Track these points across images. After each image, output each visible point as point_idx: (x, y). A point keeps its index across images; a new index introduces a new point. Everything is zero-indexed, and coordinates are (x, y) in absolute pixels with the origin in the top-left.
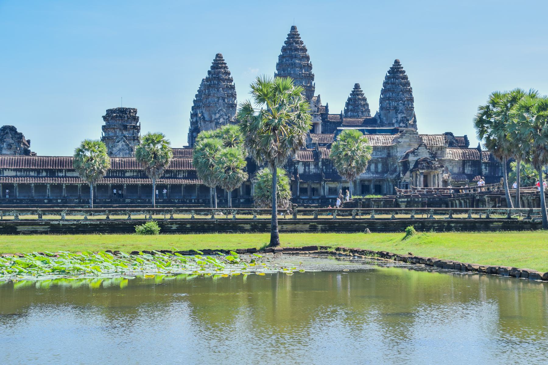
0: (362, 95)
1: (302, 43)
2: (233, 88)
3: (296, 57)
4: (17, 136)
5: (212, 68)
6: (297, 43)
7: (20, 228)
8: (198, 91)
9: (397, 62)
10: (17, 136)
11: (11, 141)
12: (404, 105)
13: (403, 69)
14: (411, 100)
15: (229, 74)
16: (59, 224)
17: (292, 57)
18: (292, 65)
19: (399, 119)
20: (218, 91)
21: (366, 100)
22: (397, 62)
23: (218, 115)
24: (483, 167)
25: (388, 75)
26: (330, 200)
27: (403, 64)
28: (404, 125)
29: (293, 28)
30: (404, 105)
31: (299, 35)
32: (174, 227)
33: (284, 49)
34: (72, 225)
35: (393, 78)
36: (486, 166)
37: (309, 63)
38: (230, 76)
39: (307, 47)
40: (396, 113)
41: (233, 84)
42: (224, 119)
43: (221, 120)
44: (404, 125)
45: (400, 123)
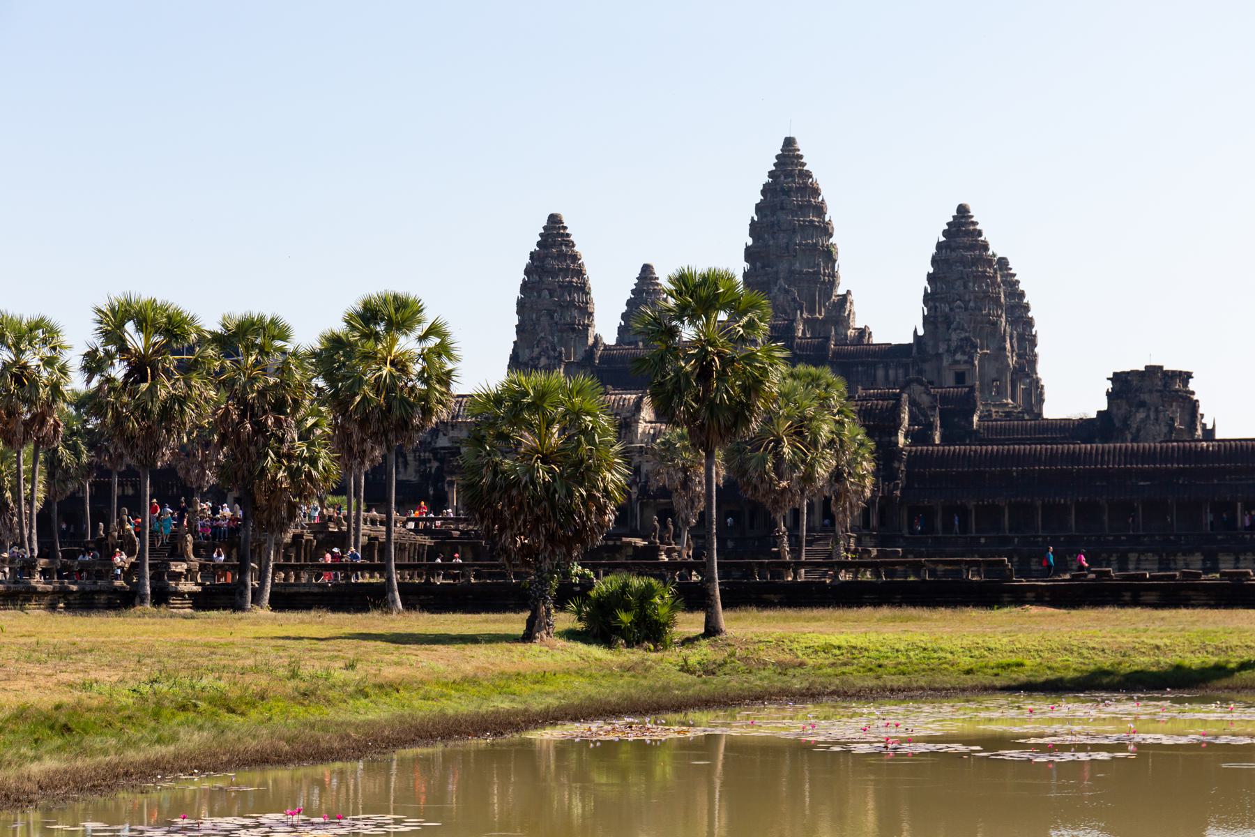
1: (808, 175)
3: (782, 208)
5: (539, 244)
9: (963, 210)
12: (966, 309)
18: (773, 225)
19: (954, 344)
20: (539, 296)
22: (963, 210)
23: (537, 350)
27: (976, 214)
28: (966, 358)
29: (789, 143)
31: (801, 157)
40: (948, 328)
44: (966, 358)
45: (955, 352)
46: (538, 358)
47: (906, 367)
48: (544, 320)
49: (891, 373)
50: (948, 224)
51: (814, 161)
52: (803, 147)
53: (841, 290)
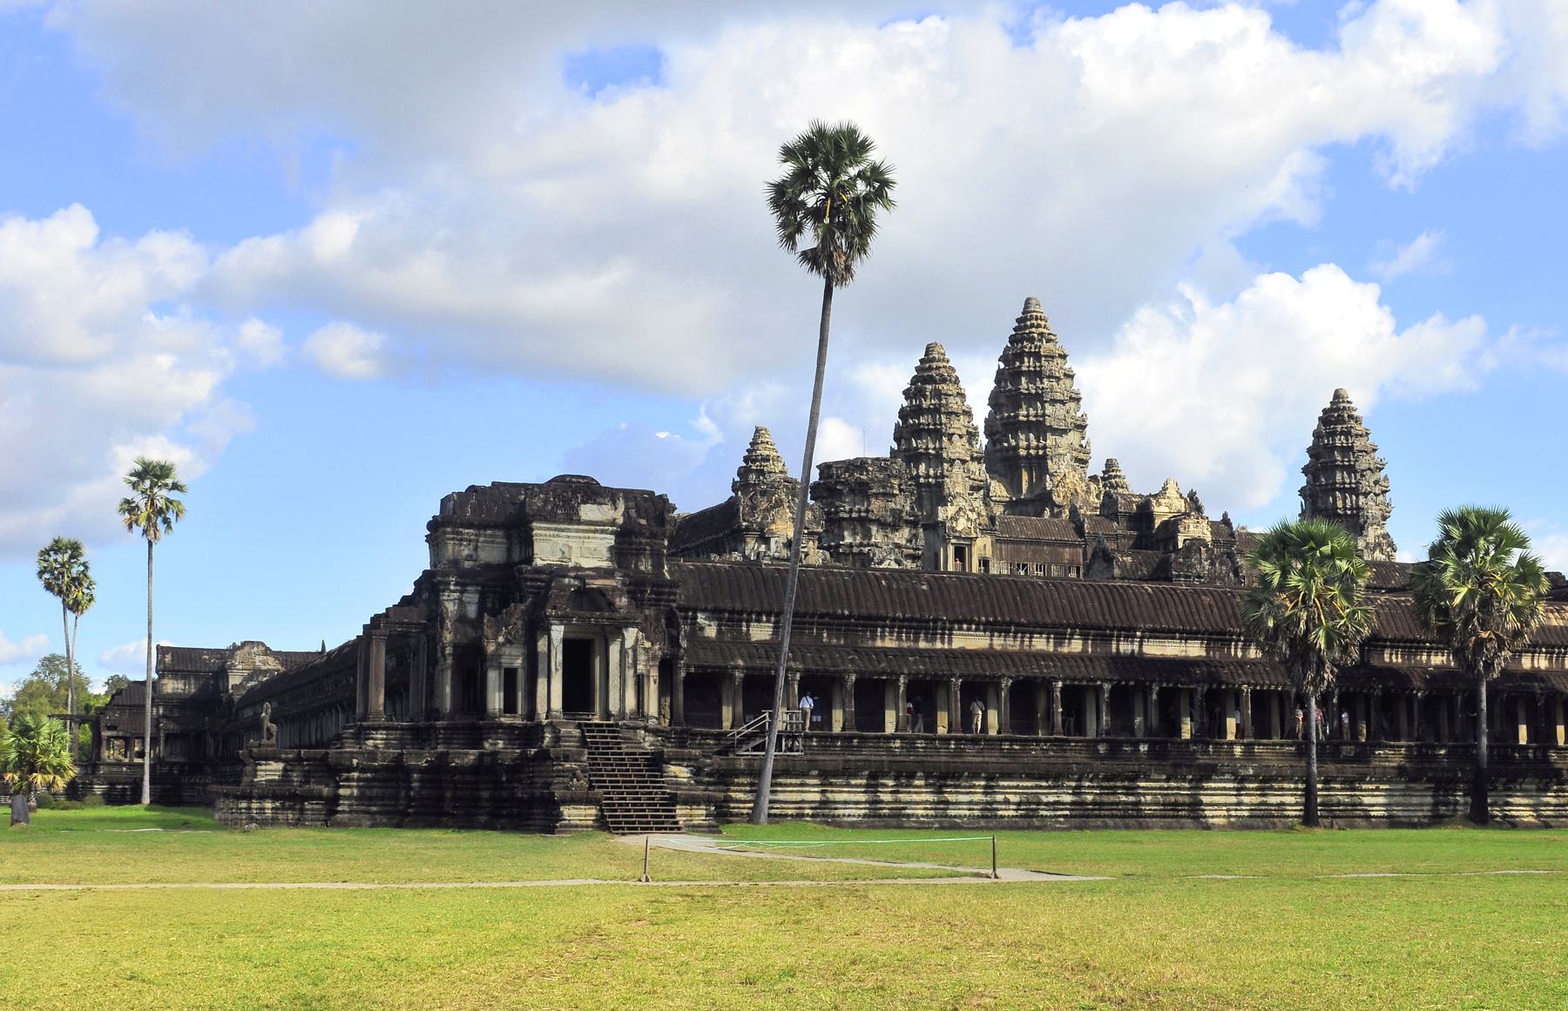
6: (1048, 341)
17: (1036, 375)
43: (961, 525)
46: (954, 518)
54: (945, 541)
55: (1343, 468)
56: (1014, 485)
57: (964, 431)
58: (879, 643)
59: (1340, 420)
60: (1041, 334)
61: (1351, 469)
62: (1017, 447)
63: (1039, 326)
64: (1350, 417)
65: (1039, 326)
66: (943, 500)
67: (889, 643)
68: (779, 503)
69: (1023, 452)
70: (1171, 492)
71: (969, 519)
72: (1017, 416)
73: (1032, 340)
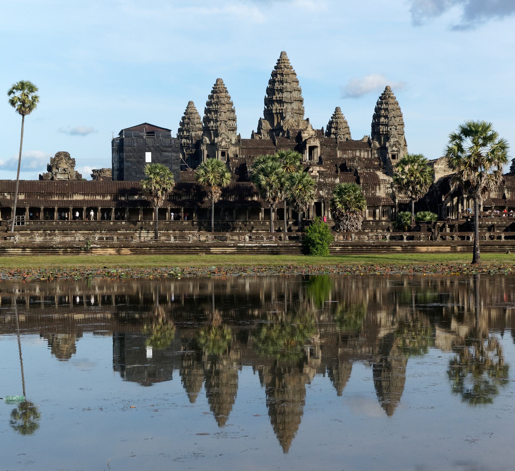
0: (343, 118)
2: (233, 111)
4: (71, 161)
5: (212, 92)
7: (213, 250)
8: (185, 113)
10: (71, 161)
11: (65, 166)
12: (396, 129)
13: (394, 95)
14: (403, 124)
15: (230, 97)
16: (244, 246)
17: (282, 82)
19: (392, 143)
21: (347, 123)
24: (506, 192)
25: (380, 100)
26: (371, 222)
30: (396, 129)
32: (338, 249)
33: (274, 74)
34: (255, 247)
35: (387, 104)
36: (508, 191)
37: (299, 86)
38: (231, 100)
39: (296, 72)
41: (233, 108)
42: (226, 142)
43: (224, 143)
46: (221, 142)
47: (368, 151)
48: (223, 125)
49: (362, 154)
50: (382, 94)
51: (295, 63)
52: (289, 56)
53: (305, 118)
54: (218, 150)
55: (384, 116)
56: (272, 124)
57: (226, 110)
58: (53, 199)
59: (385, 98)
60: (285, 66)
61: (386, 117)
62: (272, 110)
63: (284, 63)
64: (389, 97)
65: (284, 63)
66: (217, 135)
67: (56, 198)
68: (62, 159)
69: (274, 112)
70: (309, 129)
71: (226, 142)
72: (272, 98)
73: (281, 68)
